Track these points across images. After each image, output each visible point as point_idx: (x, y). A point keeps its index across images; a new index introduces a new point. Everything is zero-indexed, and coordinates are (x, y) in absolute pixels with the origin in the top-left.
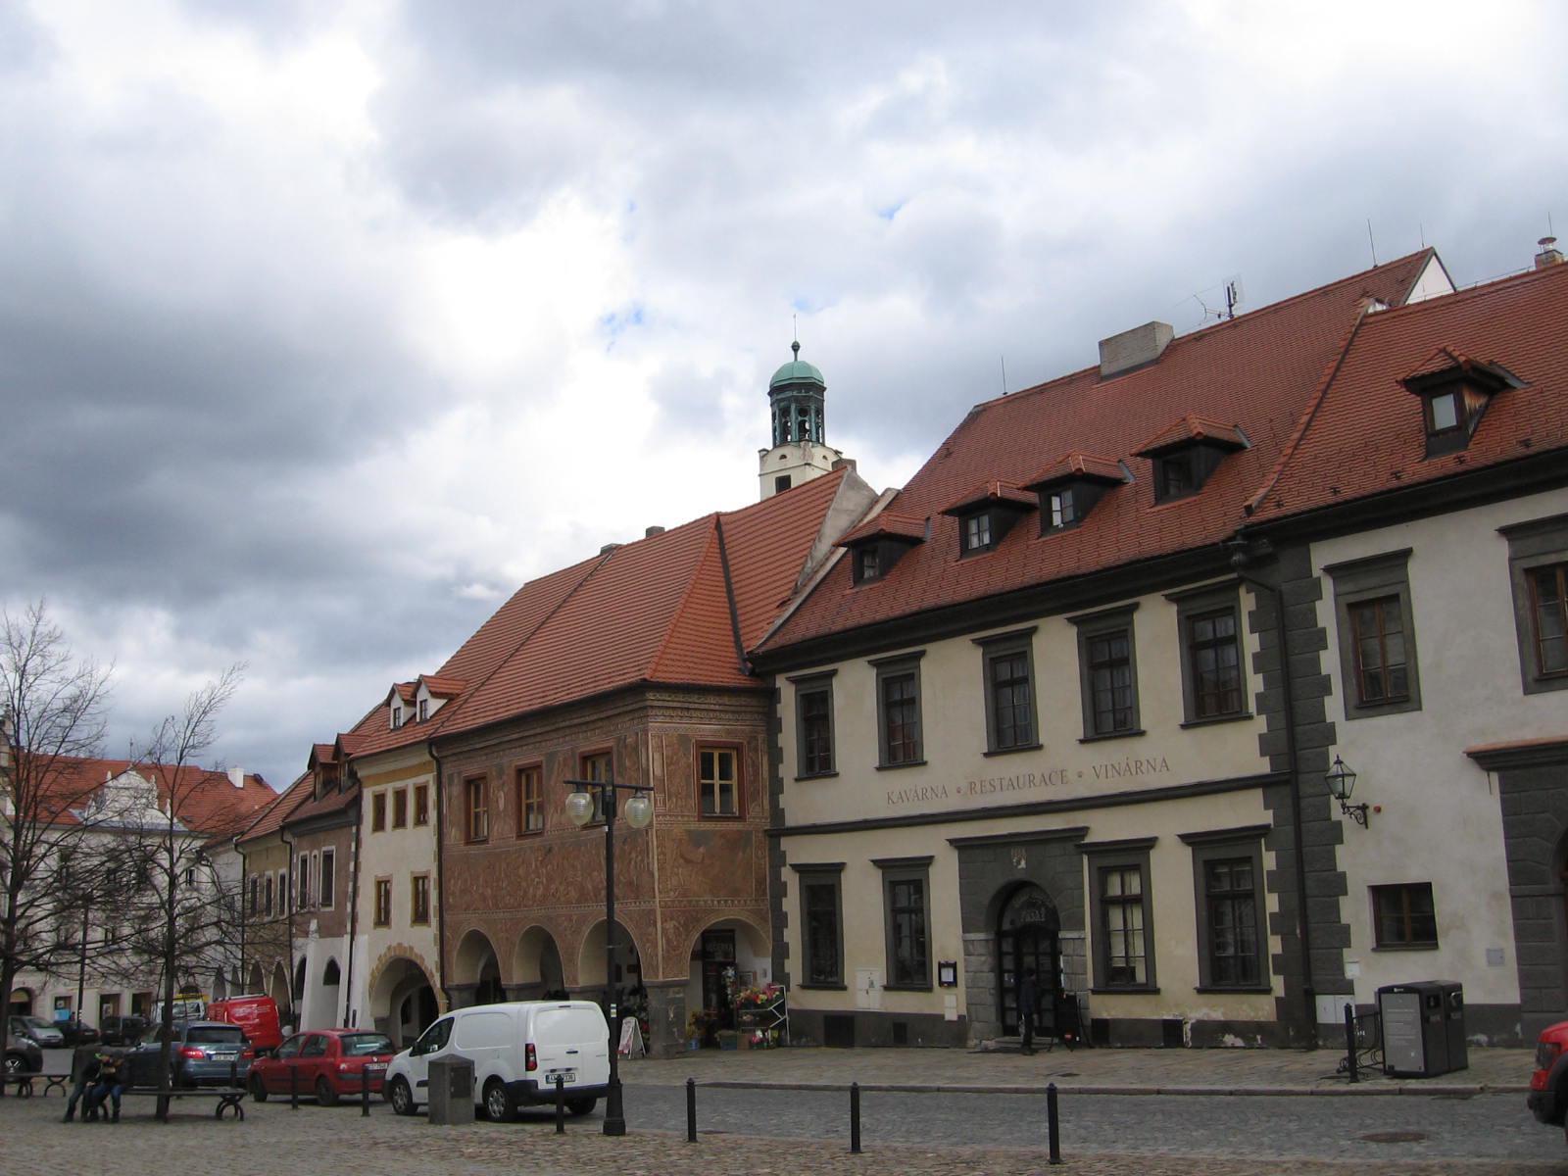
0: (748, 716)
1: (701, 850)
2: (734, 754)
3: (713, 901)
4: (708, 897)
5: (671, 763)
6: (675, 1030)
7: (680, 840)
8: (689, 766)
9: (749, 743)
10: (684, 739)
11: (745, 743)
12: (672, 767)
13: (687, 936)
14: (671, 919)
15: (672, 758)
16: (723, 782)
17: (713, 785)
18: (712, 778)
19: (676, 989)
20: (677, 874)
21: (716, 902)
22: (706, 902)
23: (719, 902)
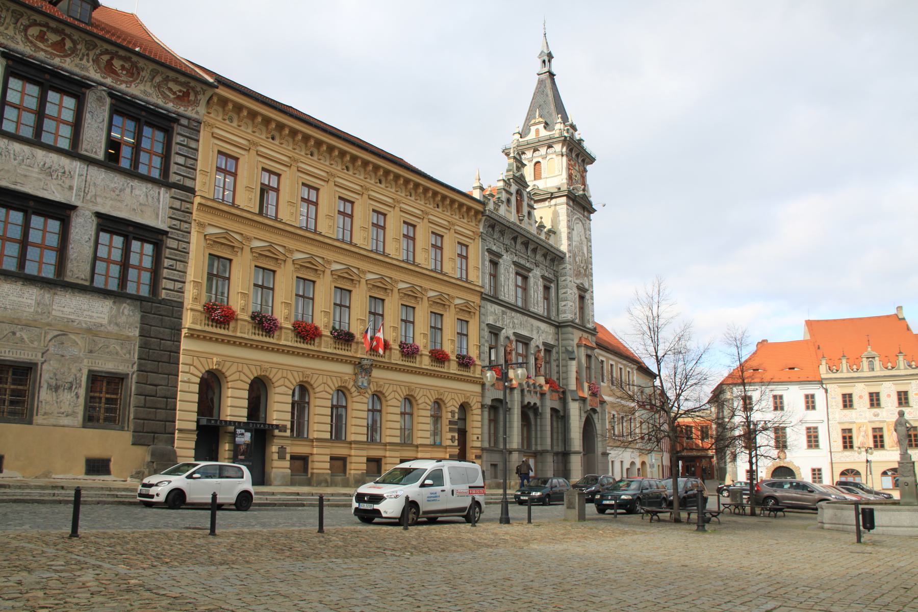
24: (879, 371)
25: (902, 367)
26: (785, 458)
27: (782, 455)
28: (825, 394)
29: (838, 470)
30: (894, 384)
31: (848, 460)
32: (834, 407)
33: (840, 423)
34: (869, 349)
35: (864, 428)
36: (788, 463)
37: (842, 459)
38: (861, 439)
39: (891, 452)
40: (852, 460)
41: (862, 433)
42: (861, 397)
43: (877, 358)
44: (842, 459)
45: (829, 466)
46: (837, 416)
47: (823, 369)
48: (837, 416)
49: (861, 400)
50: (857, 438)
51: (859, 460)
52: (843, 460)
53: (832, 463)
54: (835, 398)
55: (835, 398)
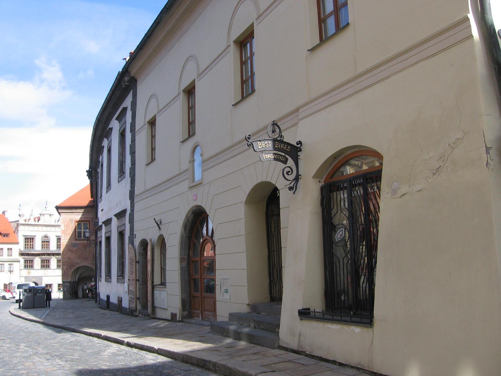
0: (92, 213)
1: (76, 248)
2: (88, 223)
3: (78, 261)
4: (77, 260)
5: (67, 226)
6: (66, 293)
7: (69, 246)
8: (73, 227)
9: (92, 220)
10: (71, 220)
11: (91, 220)
12: (67, 227)
13: (70, 270)
14: (65, 266)
15: (67, 225)
16: (78, 230)
17: (81, 232)
18: (81, 229)
19: (67, 283)
20: (68, 254)
21: (79, 261)
22: (76, 261)
23: (80, 261)
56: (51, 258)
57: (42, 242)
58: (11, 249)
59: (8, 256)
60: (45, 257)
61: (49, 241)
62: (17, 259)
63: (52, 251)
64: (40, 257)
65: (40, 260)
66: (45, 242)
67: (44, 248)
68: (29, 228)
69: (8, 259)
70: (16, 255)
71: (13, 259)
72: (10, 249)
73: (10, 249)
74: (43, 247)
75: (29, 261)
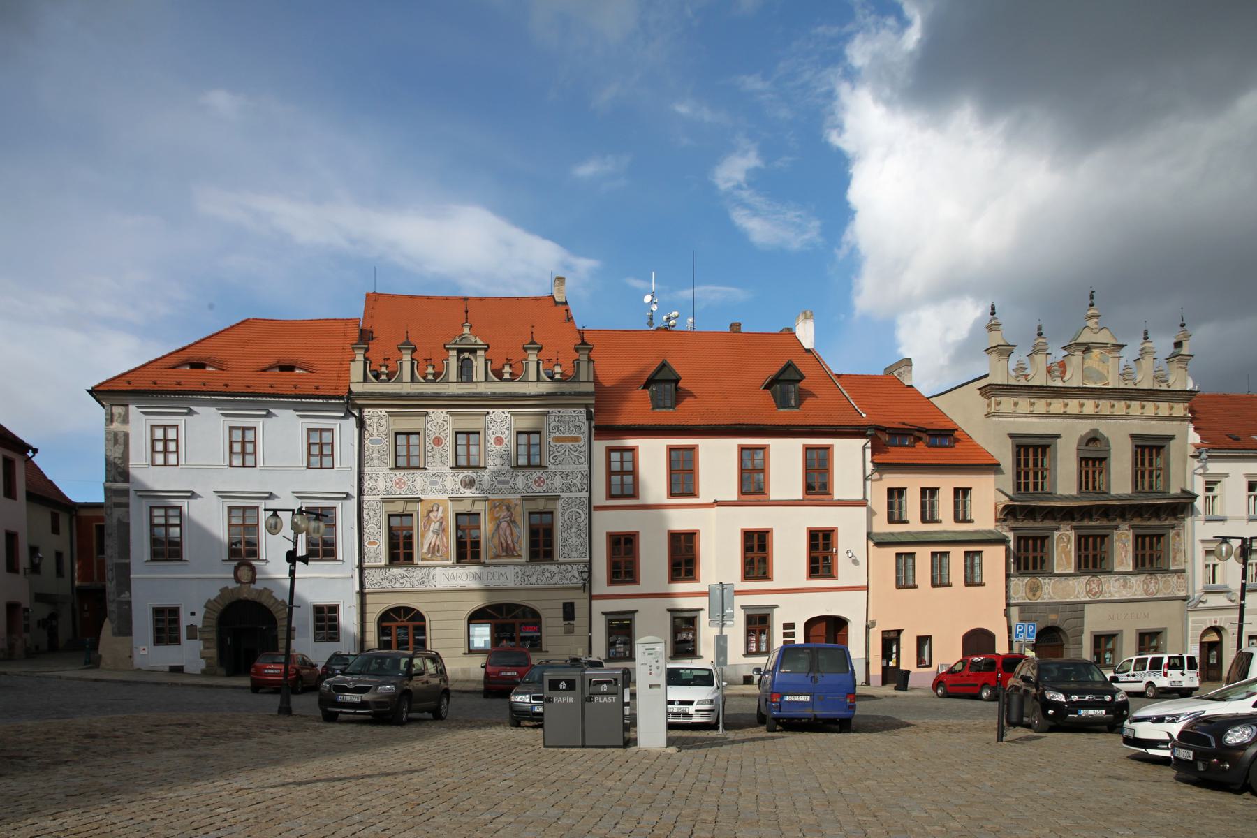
24: (479, 385)
25: (532, 375)
26: (253, 581)
27: (245, 573)
28: (356, 431)
29: (375, 610)
30: (513, 414)
31: (398, 586)
32: (376, 462)
33: (385, 500)
34: (466, 331)
35: (440, 514)
36: (260, 592)
37: (386, 583)
38: (430, 538)
39: (492, 569)
40: (408, 587)
41: (434, 526)
42: (437, 441)
43: (481, 353)
44: (386, 583)
45: (355, 600)
46: (381, 485)
47: (356, 370)
48: (381, 485)
49: (437, 449)
50: (423, 536)
51: (422, 588)
52: (387, 586)
53: (362, 594)
54: (379, 441)
55: (379, 441)
56: (1117, 528)
57: (1081, 459)
58: (966, 491)
59: (957, 520)
60: (1092, 523)
61: (1102, 460)
62: (990, 532)
63: (1118, 498)
64: (1074, 524)
65: (1072, 535)
66: (1090, 463)
67: (1087, 488)
68: (1033, 404)
69: (954, 532)
70: (984, 516)
71: (976, 532)
72: (962, 494)
73: (962, 494)
74: (1083, 483)
75: (1030, 542)
